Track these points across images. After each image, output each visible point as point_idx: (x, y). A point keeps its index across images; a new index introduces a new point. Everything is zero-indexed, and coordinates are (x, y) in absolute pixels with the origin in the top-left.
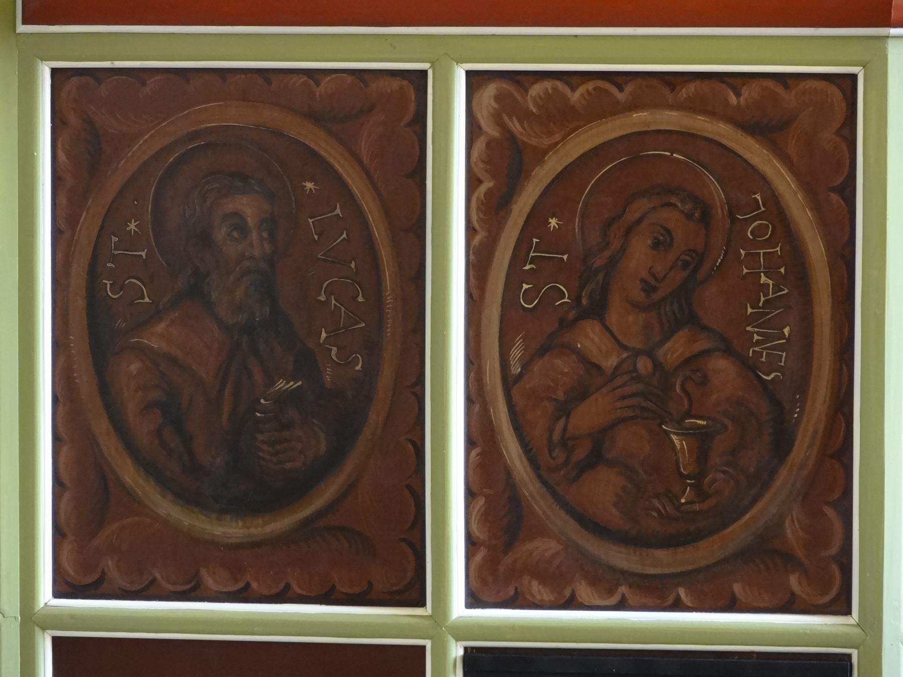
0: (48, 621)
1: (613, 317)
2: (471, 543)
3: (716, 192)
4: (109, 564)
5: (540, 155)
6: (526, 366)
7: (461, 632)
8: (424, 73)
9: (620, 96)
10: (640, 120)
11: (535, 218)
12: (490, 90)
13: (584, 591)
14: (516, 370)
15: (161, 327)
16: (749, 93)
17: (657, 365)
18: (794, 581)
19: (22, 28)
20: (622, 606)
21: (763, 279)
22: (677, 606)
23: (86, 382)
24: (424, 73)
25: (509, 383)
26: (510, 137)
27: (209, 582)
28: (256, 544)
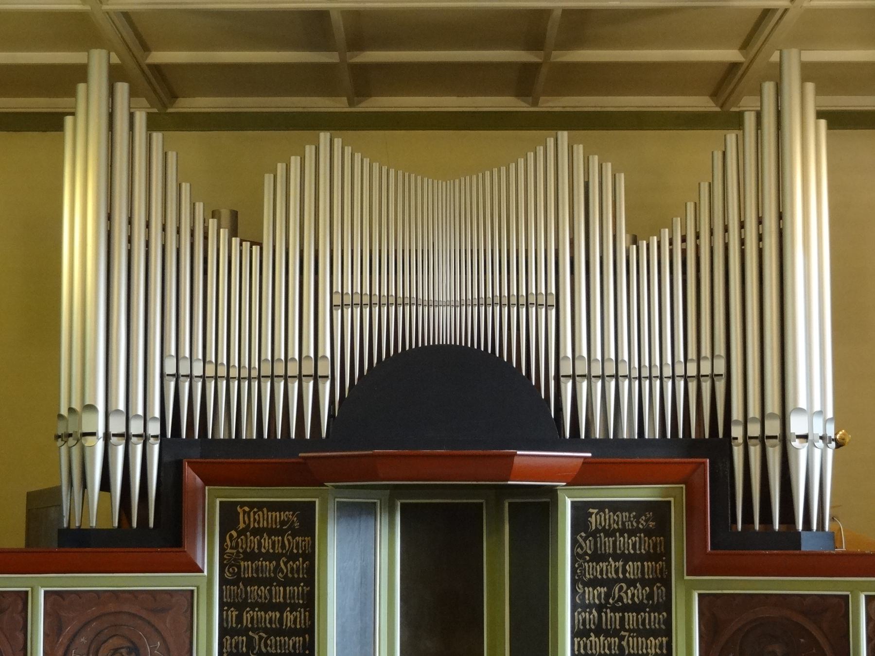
8: (847, 596)
19: (686, 578)
24: (847, 596)
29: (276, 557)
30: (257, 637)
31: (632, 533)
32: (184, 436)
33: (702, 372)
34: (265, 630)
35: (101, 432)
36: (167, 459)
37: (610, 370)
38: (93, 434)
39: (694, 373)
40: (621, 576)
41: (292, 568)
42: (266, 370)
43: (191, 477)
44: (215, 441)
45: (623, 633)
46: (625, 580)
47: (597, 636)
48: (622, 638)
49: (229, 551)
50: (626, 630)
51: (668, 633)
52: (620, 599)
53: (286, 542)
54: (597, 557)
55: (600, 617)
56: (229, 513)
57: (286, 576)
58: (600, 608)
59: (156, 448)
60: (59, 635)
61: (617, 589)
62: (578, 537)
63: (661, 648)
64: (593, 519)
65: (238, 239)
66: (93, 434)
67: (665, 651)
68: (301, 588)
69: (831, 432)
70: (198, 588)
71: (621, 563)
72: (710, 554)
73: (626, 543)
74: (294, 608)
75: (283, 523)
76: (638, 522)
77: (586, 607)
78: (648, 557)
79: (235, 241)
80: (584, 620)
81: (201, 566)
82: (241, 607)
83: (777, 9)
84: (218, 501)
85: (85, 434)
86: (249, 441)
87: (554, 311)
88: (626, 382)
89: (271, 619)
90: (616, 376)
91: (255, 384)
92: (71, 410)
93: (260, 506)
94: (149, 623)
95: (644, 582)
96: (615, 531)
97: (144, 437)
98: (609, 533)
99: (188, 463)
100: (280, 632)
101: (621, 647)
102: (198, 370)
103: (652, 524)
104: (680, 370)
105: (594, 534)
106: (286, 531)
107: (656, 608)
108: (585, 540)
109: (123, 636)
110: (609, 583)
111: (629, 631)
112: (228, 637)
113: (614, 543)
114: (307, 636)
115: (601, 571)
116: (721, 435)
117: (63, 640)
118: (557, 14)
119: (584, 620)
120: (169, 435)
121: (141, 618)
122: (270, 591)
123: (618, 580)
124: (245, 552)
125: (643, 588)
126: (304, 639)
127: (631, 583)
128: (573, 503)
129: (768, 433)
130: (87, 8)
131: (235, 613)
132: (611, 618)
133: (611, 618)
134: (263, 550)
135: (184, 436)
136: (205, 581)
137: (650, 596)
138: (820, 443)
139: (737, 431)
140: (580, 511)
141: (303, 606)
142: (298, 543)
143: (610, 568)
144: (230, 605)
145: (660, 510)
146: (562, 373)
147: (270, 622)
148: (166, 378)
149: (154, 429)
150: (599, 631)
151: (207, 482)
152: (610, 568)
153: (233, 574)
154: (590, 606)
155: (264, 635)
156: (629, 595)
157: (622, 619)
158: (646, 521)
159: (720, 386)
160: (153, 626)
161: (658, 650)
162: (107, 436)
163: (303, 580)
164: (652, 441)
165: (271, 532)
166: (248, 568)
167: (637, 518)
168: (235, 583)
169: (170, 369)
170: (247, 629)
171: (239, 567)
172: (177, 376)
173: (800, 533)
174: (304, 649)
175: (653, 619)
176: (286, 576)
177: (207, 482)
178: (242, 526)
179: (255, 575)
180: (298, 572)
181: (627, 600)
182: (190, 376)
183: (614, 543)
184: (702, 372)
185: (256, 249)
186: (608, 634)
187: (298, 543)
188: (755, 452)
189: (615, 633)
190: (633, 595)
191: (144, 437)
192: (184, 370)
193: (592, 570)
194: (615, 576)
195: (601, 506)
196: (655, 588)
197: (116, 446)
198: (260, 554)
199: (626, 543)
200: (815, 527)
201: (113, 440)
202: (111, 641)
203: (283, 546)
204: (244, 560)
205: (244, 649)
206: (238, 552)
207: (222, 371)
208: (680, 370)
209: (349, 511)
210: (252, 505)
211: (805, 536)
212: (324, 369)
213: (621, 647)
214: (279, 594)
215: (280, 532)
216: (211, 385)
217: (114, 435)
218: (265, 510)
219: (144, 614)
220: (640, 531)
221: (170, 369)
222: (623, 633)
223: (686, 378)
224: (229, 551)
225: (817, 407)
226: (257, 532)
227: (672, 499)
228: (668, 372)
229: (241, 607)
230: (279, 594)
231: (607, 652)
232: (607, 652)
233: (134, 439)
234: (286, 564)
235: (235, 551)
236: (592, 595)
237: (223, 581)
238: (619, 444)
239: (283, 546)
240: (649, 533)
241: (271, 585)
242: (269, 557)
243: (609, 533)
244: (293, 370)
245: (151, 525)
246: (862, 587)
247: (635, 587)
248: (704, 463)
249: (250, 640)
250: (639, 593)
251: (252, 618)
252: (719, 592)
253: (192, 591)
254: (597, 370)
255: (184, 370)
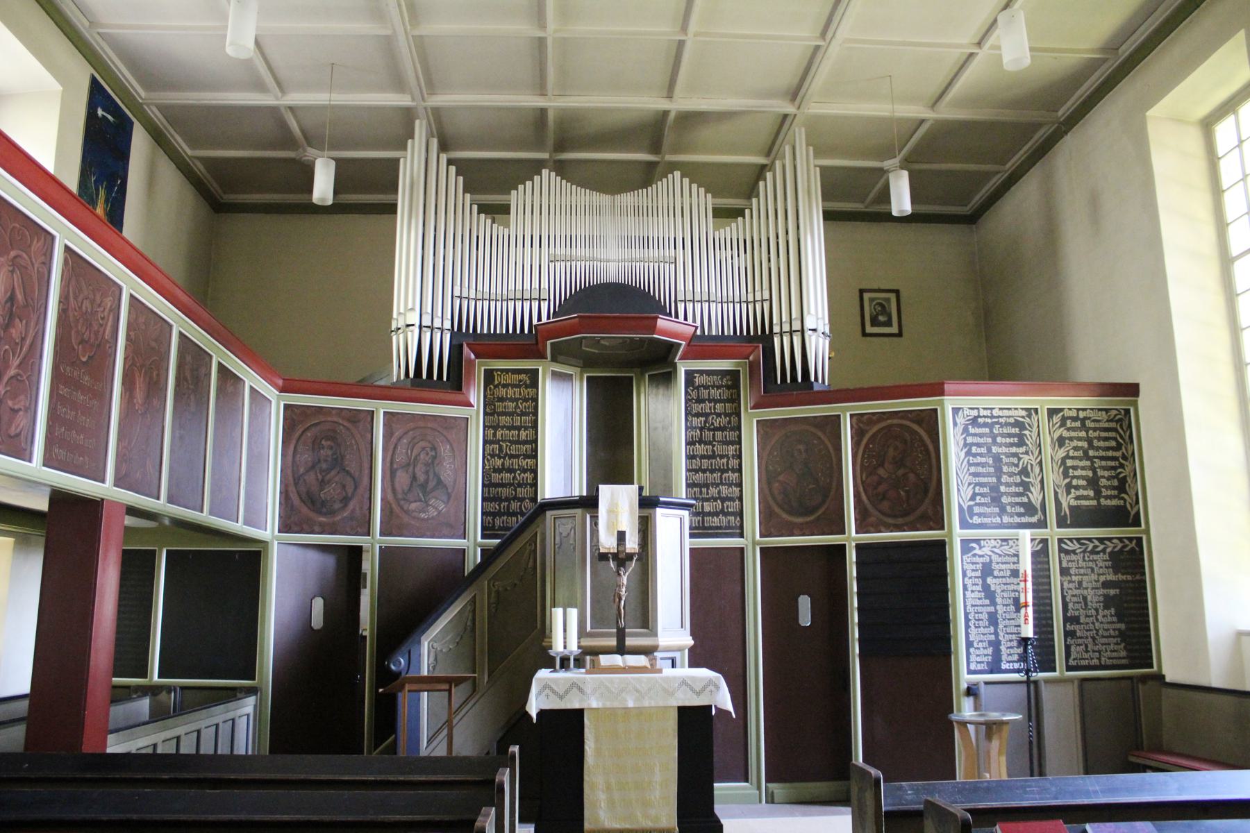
0: (759, 543)
1: (886, 465)
2: (856, 520)
3: (908, 437)
4: (772, 530)
5: (867, 431)
6: (867, 478)
7: (854, 540)
8: (840, 415)
9: (885, 417)
10: (889, 422)
11: (867, 446)
12: (855, 418)
13: (883, 529)
14: (864, 478)
15: (783, 475)
16: (913, 414)
17: (896, 476)
18: (931, 523)
20: (891, 532)
21: (920, 455)
22: (904, 531)
23: (765, 486)
25: (863, 482)
26: (860, 427)
27: (795, 532)
28: (807, 523)
29: (516, 400)
30: (505, 445)
31: (718, 387)
32: (464, 331)
33: (756, 299)
34: (510, 441)
35: (417, 324)
36: (454, 343)
37: (705, 297)
38: (413, 325)
39: (752, 300)
40: (713, 411)
41: (525, 407)
42: (511, 296)
43: (468, 353)
44: (482, 334)
45: (714, 443)
46: (715, 413)
47: (700, 444)
48: (714, 446)
49: (489, 396)
50: (716, 441)
51: (740, 443)
52: (713, 424)
53: (522, 391)
54: (699, 401)
55: (701, 434)
56: (489, 375)
57: (521, 411)
58: (701, 429)
59: (448, 336)
60: (391, 437)
61: (711, 419)
62: (689, 390)
63: (736, 451)
64: (697, 380)
65: (496, 225)
66: (413, 325)
67: (738, 453)
68: (531, 417)
69: (827, 331)
70: (471, 416)
71: (713, 404)
72: (763, 396)
73: (715, 393)
74: (526, 428)
75: (520, 381)
76: (722, 381)
77: (693, 428)
78: (728, 401)
79: (495, 226)
80: (692, 436)
81: (472, 402)
82: (496, 428)
83: (791, 115)
84: (483, 369)
85: (408, 326)
86: (501, 334)
87: (674, 265)
88: (715, 304)
89: (513, 435)
90: (709, 301)
91: (505, 304)
92: (399, 314)
93: (507, 371)
94: (442, 434)
95: (726, 415)
96: (709, 386)
97: (441, 329)
98: (706, 387)
99: (468, 345)
100: (518, 442)
101: (713, 451)
102: (472, 295)
103: (730, 383)
104: (744, 299)
105: (698, 388)
106: (522, 385)
107: (732, 429)
108: (692, 391)
109: (429, 442)
110: (706, 415)
111: (718, 442)
112: (488, 445)
113: (709, 393)
114: (534, 445)
115: (702, 408)
116: (767, 333)
117: (394, 440)
118: (672, 116)
119: (692, 436)
120: (456, 330)
121: (439, 431)
122: (512, 419)
123: (711, 414)
124: (498, 397)
125: (725, 418)
126: (532, 446)
127: (719, 415)
128: (686, 371)
129: (793, 329)
130: (414, 104)
131: (492, 431)
132: (708, 435)
133: (708, 435)
134: (509, 396)
135: (464, 331)
136: (475, 412)
137: (729, 422)
138: (822, 335)
139: (776, 329)
140: (690, 375)
141: (532, 427)
142: (528, 393)
143: (707, 407)
144: (489, 427)
145: (734, 375)
146: (678, 299)
147: (513, 437)
148: (455, 298)
149: (447, 325)
150: (701, 442)
151: (477, 357)
152: (707, 407)
153: (491, 410)
154: (695, 428)
155: (509, 444)
156: (718, 422)
157: (714, 435)
158: (727, 381)
159: (766, 305)
160: (445, 436)
161: (734, 453)
162: (421, 327)
163: (532, 413)
164: (729, 336)
165: (514, 386)
166: (500, 406)
167: (722, 379)
168: (492, 415)
169: (457, 293)
170: (499, 441)
171: (495, 406)
172: (461, 298)
173: (812, 383)
174: (532, 451)
175: (731, 435)
176: (521, 411)
177: (477, 357)
178: (496, 382)
179: (504, 410)
180: (529, 409)
181: (716, 425)
182: (468, 298)
183: (709, 393)
184: (756, 299)
185: (506, 231)
186: (706, 443)
187: (528, 393)
188: (786, 339)
189: (710, 443)
190: (720, 422)
191: (441, 329)
192: (465, 294)
193: (697, 408)
194: (709, 411)
195: (701, 372)
196: (732, 418)
197: (425, 332)
198: (507, 398)
199: (715, 393)
200: (820, 381)
201: (424, 329)
202: (421, 443)
203: (520, 394)
204: (497, 401)
205: (497, 452)
206: (494, 397)
207: (486, 296)
208: (744, 299)
209: (556, 375)
210: (502, 371)
211: (815, 384)
212: (544, 295)
213: (713, 451)
214: (517, 421)
215: (518, 386)
216: (479, 304)
217: (424, 327)
218: (510, 374)
219: (439, 429)
220: (722, 386)
221: (457, 293)
222: (714, 443)
223: (747, 303)
224: (489, 396)
225: (820, 315)
226: (505, 386)
227: (741, 369)
228: (737, 299)
229: (496, 428)
230: (517, 421)
231: (706, 453)
232: (706, 453)
233: (436, 330)
234: (521, 404)
235: (492, 397)
236: (697, 422)
237: (485, 414)
238: (711, 337)
239: (520, 394)
240: (728, 387)
241: (513, 416)
242: (512, 400)
243: (706, 387)
244: (527, 296)
245: (445, 379)
246: (848, 409)
247: (721, 418)
248: (758, 346)
249: (501, 447)
250: (723, 421)
251: (502, 435)
252: (768, 418)
253: (468, 419)
254: (698, 298)
255: (465, 294)
